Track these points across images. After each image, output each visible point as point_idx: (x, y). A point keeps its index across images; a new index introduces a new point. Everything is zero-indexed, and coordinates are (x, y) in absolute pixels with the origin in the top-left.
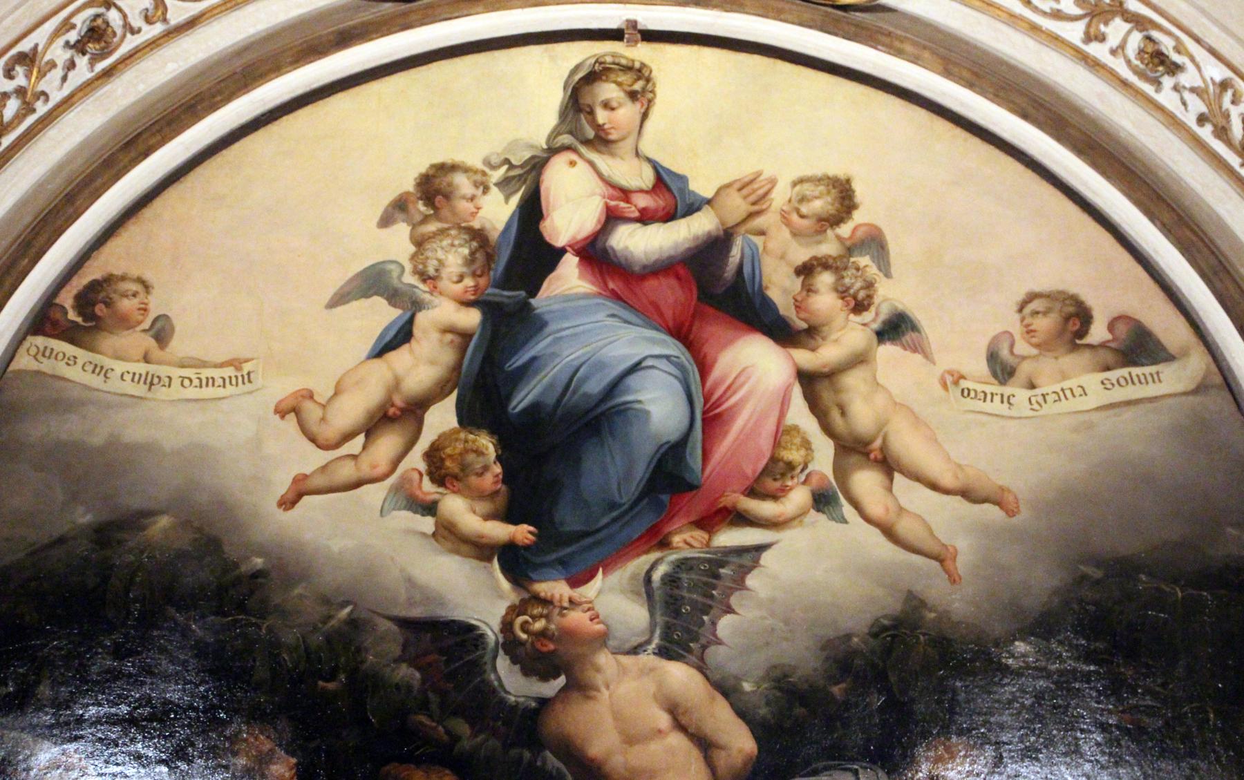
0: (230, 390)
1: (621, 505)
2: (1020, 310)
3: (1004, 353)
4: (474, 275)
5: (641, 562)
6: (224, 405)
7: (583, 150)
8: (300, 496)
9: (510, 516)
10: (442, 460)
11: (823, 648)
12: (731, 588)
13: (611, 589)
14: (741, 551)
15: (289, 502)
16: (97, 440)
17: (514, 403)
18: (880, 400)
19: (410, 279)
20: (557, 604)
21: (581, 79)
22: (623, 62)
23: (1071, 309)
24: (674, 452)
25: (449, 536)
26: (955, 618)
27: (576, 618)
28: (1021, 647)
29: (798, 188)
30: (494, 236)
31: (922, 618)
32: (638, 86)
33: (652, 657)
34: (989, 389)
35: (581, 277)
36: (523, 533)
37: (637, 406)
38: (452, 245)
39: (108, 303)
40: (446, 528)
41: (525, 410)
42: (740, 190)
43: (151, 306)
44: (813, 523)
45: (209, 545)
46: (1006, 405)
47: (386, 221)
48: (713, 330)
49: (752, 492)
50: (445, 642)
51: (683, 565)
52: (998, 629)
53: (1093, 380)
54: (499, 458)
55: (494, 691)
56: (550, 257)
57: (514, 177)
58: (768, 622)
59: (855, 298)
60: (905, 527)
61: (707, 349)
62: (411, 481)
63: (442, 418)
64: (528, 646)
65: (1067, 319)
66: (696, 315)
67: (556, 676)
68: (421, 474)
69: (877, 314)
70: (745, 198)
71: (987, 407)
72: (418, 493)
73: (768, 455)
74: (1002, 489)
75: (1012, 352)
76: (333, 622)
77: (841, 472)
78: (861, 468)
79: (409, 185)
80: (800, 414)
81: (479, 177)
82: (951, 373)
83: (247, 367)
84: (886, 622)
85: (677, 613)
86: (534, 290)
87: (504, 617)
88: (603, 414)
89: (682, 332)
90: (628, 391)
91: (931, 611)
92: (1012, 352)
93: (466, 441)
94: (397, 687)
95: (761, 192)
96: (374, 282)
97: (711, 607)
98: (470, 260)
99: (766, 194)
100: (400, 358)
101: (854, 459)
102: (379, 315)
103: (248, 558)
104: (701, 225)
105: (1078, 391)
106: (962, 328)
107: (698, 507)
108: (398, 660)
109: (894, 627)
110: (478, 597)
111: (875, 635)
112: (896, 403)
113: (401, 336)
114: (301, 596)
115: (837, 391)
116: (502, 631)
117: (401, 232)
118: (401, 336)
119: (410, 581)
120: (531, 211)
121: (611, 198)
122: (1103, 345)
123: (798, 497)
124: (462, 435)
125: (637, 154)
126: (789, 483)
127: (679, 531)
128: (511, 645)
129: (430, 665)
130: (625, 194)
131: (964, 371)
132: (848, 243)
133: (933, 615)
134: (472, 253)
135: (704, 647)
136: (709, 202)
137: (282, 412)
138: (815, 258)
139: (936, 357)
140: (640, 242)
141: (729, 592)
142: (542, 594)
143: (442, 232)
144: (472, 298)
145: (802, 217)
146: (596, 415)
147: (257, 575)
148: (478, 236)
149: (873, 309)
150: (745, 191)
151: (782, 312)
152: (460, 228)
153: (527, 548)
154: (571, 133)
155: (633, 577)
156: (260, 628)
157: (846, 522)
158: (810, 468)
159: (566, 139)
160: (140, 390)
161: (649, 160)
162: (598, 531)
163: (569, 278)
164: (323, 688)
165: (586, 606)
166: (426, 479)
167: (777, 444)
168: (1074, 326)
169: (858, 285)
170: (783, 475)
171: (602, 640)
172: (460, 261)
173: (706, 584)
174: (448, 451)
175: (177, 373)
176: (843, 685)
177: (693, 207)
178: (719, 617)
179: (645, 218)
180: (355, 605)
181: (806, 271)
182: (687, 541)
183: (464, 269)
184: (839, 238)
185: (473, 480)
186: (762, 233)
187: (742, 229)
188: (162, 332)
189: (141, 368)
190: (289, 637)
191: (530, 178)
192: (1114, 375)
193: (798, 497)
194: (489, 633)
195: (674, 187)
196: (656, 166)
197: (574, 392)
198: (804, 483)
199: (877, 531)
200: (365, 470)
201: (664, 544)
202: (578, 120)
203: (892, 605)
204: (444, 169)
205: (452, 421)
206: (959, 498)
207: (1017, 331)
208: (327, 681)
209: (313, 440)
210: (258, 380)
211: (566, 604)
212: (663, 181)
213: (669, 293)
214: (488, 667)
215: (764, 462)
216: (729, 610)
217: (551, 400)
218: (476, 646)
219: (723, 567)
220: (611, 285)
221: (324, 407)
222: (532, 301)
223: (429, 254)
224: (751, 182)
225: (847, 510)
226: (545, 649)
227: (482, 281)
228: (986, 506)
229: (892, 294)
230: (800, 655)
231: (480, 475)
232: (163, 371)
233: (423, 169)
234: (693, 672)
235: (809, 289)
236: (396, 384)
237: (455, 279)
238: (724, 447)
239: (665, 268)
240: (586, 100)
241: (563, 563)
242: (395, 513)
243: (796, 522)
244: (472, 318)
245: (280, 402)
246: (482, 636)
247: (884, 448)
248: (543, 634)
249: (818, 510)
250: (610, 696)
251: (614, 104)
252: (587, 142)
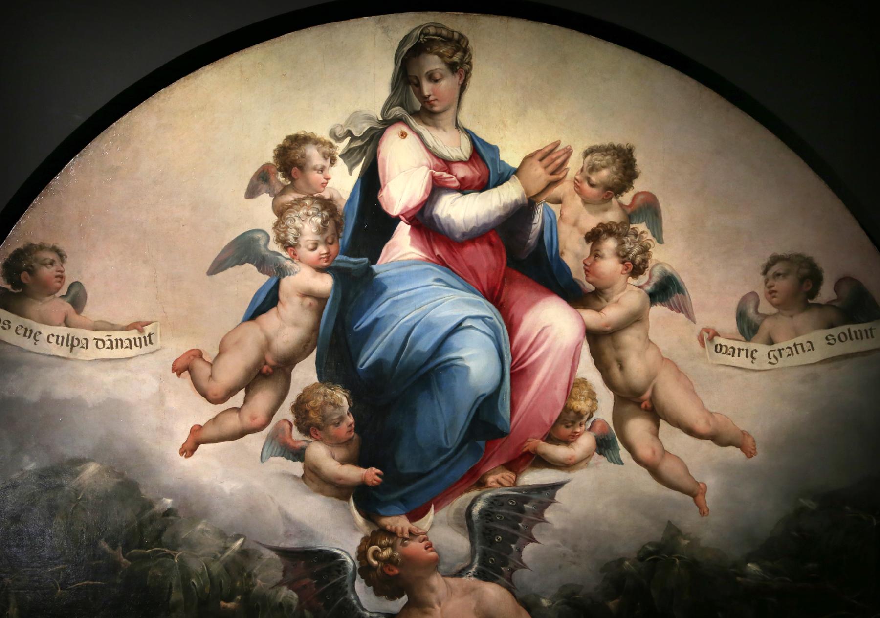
0: (135, 351)
1: (449, 450)
2: (765, 273)
3: (751, 311)
4: (326, 243)
5: (462, 501)
6: (132, 364)
7: (412, 122)
8: (197, 444)
9: (361, 461)
10: (307, 412)
11: (602, 570)
12: (533, 520)
13: (441, 522)
14: (541, 489)
15: (189, 450)
16: (33, 396)
17: (361, 361)
18: (651, 354)
19: (274, 247)
20: (399, 535)
21: (409, 50)
22: (444, 33)
23: (805, 271)
24: (488, 403)
25: (315, 478)
26: (703, 543)
27: (415, 546)
28: (752, 567)
29: (589, 158)
30: (341, 205)
32: (456, 59)
33: (473, 579)
34: (737, 345)
35: (413, 243)
36: (372, 475)
37: (459, 362)
38: (308, 215)
39: (32, 272)
40: (312, 472)
41: (369, 368)
42: (541, 160)
43: (66, 273)
44: (596, 464)
45: (128, 489)
46: (750, 358)
47: (252, 192)
48: (519, 293)
49: (550, 438)
50: (313, 565)
51: (495, 501)
53: (818, 336)
54: (351, 409)
55: (354, 607)
56: (388, 224)
57: (355, 149)
58: (560, 549)
59: (633, 261)
60: (668, 467)
61: (515, 310)
62: (283, 430)
63: (305, 374)
64: (379, 571)
65: (802, 280)
66: (506, 279)
67: (402, 595)
68: (290, 424)
69: (650, 277)
70: (545, 167)
71: (735, 361)
72: (289, 441)
73: (562, 405)
74: (743, 433)
75: (757, 312)
76: (228, 553)
77: (619, 419)
78: (635, 416)
79: (269, 157)
80: (588, 370)
81: (326, 149)
82: (707, 330)
83: (148, 329)
84: (651, 548)
85: (492, 543)
86: (374, 259)
87: (360, 547)
88: (432, 369)
89: (494, 295)
90: (451, 349)
92: (757, 312)
93: (325, 395)
94: (280, 604)
95: (559, 161)
96: (244, 250)
97: (517, 537)
98: (322, 229)
99: (564, 162)
100: (270, 320)
101: (629, 408)
102: (250, 281)
103: (160, 499)
104: (509, 194)
105: (807, 346)
107: (506, 450)
108: (280, 584)
110: (339, 531)
111: (641, 559)
112: (663, 359)
113: (269, 301)
114: (203, 532)
115: (617, 347)
116: (358, 558)
117: (265, 200)
118: (269, 301)
119: (287, 518)
120: (371, 182)
121: (436, 168)
122: (829, 304)
123: (585, 442)
124: (322, 390)
125: (457, 126)
126: (578, 430)
127: (493, 472)
128: (365, 570)
129: (305, 587)
130: (447, 164)
131: (718, 328)
132: (629, 210)
133: (687, 542)
134: (324, 222)
135: (512, 571)
136: (516, 172)
137: (178, 369)
138: (601, 225)
139: (697, 316)
140: (461, 211)
141: (531, 524)
142: (389, 527)
143: (299, 202)
144: (325, 264)
145: (592, 185)
146: (428, 370)
147: (168, 513)
148: (328, 205)
149: (647, 272)
150: (545, 162)
151: (574, 276)
152: (313, 198)
153: (375, 488)
154: (401, 105)
155: (458, 511)
156: (173, 558)
157: (621, 463)
158: (596, 416)
159: (397, 111)
160: (63, 351)
161: (467, 132)
162: (430, 472)
163: (403, 245)
164: (224, 608)
165: (422, 537)
166: (295, 429)
167: (569, 395)
168: (808, 287)
169: (636, 250)
170: (574, 423)
171: (434, 565)
172: (314, 230)
173: (514, 517)
174: (311, 403)
175: (92, 335)
176: (617, 601)
177: (503, 176)
178: (524, 545)
179: (464, 187)
180: (245, 537)
181: (594, 237)
182: (499, 481)
183: (318, 238)
184: (621, 205)
185: (332, 429)
186: (559, 201)
187: (543, 198)
188: (77, 298)
189: (62, 331)
190: (196, 565)
191: (369, 149)
192: (835, 332)
193: (585, 442)
194: (349, 560)
195: (487, 157)
196: (473, 139)
197: (409, 351)
198: (590, 430)
199: (645, 471)
200: (247, 421)
201: (481, 484)
202: (408, 90)
203: (657, 534)
204: (298, 141)
205: (314, 378)
206: (709, 442)
207: (761, 291)
208: (227, 601)
209: (204, 394)
210: (158, 342)
211: (406, 536)
212: (481, 153)
213: (483, 258)
214: (349, 589)
215: (559, 411)
216: (532, 540)
217: (391, 358)
218: (339, 571)
219: (526, 503)
220: (437, 252)
221: (211, 365)
222: (374, 267)
223: (289, 223)
224: (551, 152)
225: (623, 453)
226: (391, 573)
227: (333, 249)
228: (731, 449)
229: (665, 257)
230: (584, 575)
231: (337, 425)
232: (81, 333)
233: (280, 141)
234: (504, 591)
235: (596, 254)
236: (268, 344)
237: (311, 246)
238: (528, 398)
239: (481, 235)
240: (413, 72)
241: (403, 500)
242: (273, 459)
243: (583, 464)
244: (325, 283)
245: (176, 361)
246: (344, 562)
247: (653, 398)
248: (390, 561)
249: (600, 454)
250: (442, 612)
251: (437, 76)
252: (415, 114)
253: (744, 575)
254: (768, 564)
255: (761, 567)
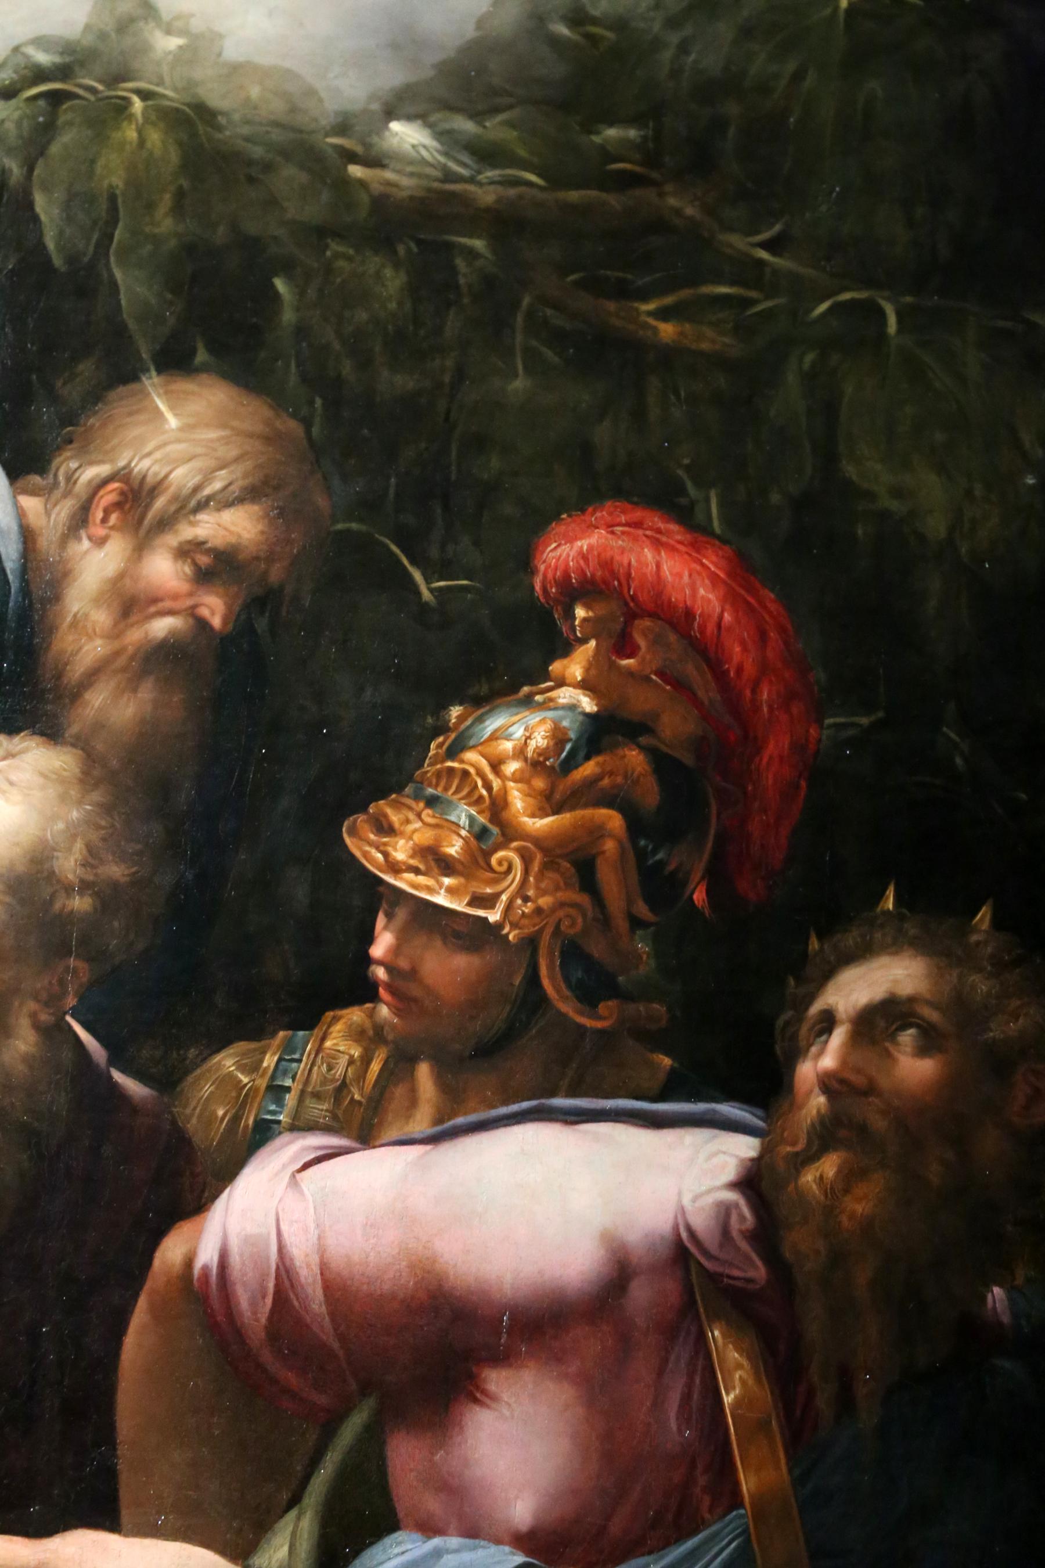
26: (232, 51)
28: (406, 135)
31: (146, 48)
52: (346, 87)
84: (43, 58)
91: (169, 32)
109: (63, 72)
133: (174, 43)
253: (374, 161)
254: (466, 126)
255: (440, 135)
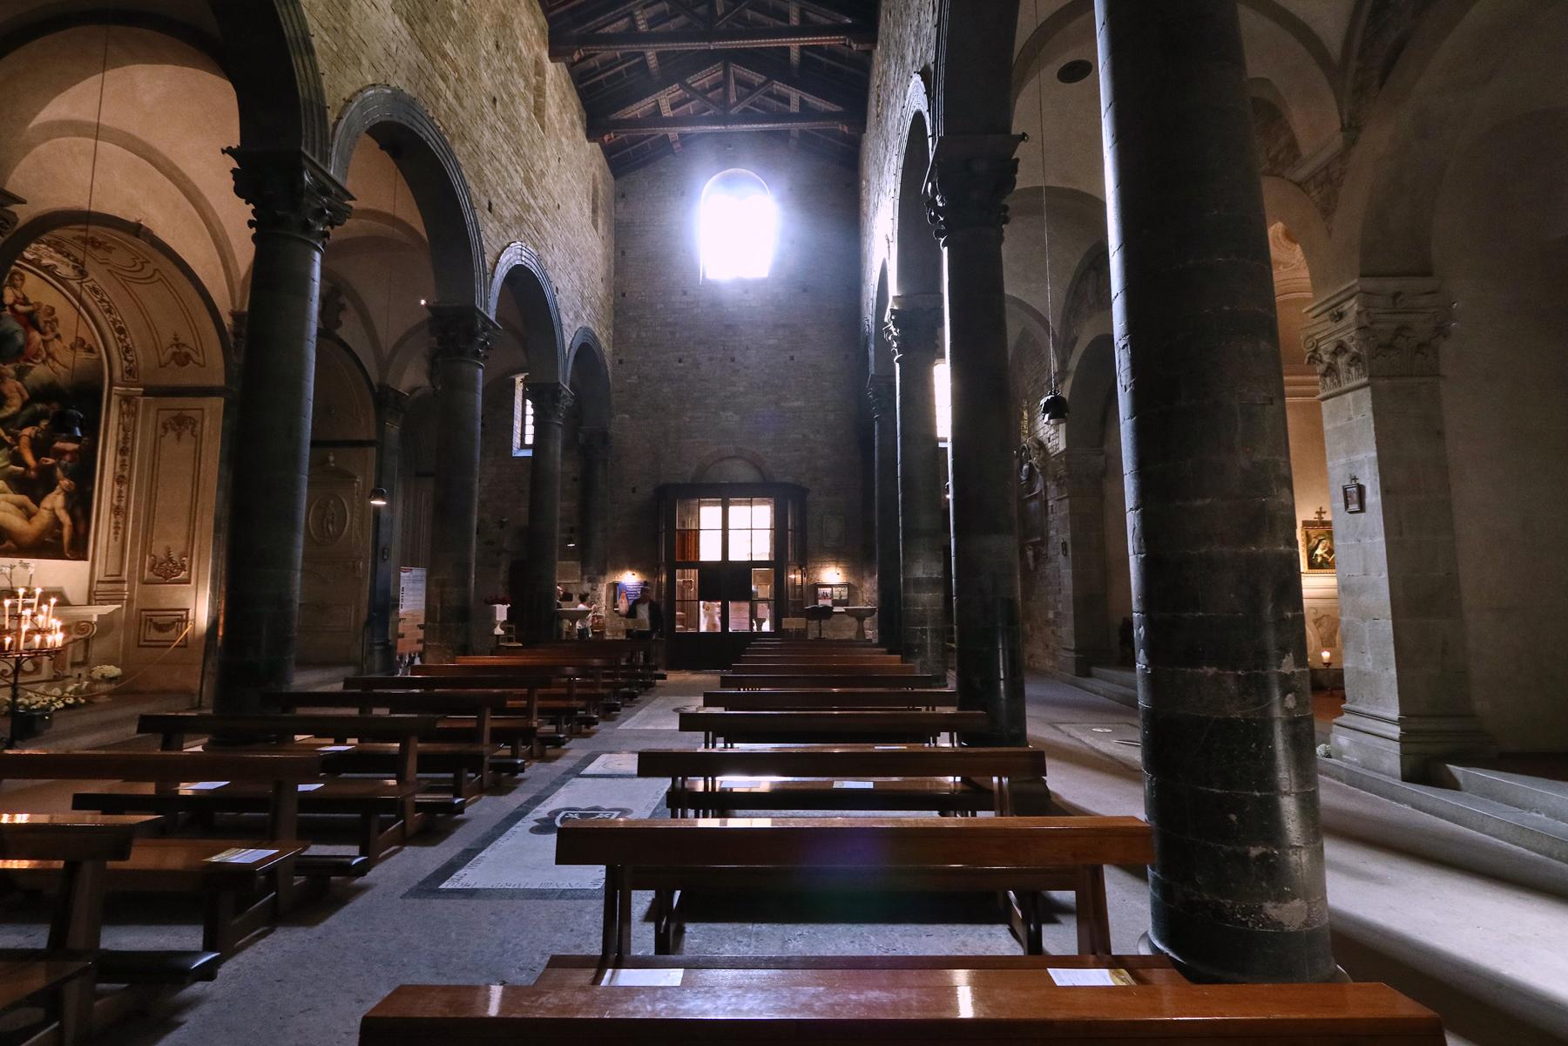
104: (29, 308)
106: (68, 340)
212: (25, 298)
229: (59, 330)
